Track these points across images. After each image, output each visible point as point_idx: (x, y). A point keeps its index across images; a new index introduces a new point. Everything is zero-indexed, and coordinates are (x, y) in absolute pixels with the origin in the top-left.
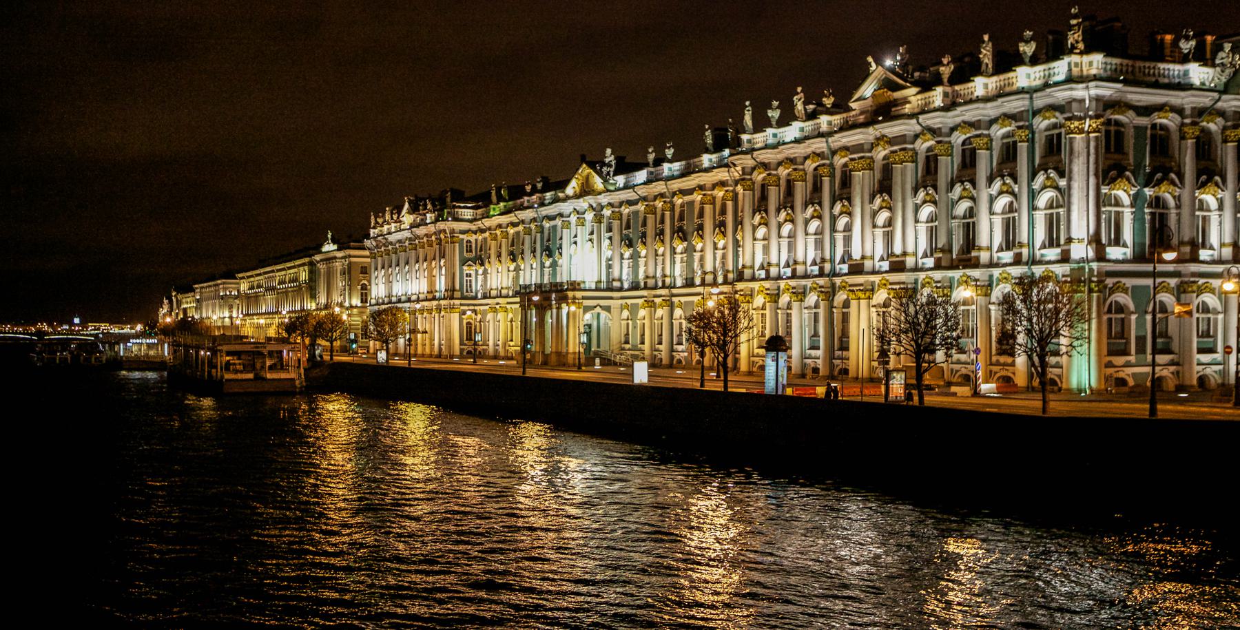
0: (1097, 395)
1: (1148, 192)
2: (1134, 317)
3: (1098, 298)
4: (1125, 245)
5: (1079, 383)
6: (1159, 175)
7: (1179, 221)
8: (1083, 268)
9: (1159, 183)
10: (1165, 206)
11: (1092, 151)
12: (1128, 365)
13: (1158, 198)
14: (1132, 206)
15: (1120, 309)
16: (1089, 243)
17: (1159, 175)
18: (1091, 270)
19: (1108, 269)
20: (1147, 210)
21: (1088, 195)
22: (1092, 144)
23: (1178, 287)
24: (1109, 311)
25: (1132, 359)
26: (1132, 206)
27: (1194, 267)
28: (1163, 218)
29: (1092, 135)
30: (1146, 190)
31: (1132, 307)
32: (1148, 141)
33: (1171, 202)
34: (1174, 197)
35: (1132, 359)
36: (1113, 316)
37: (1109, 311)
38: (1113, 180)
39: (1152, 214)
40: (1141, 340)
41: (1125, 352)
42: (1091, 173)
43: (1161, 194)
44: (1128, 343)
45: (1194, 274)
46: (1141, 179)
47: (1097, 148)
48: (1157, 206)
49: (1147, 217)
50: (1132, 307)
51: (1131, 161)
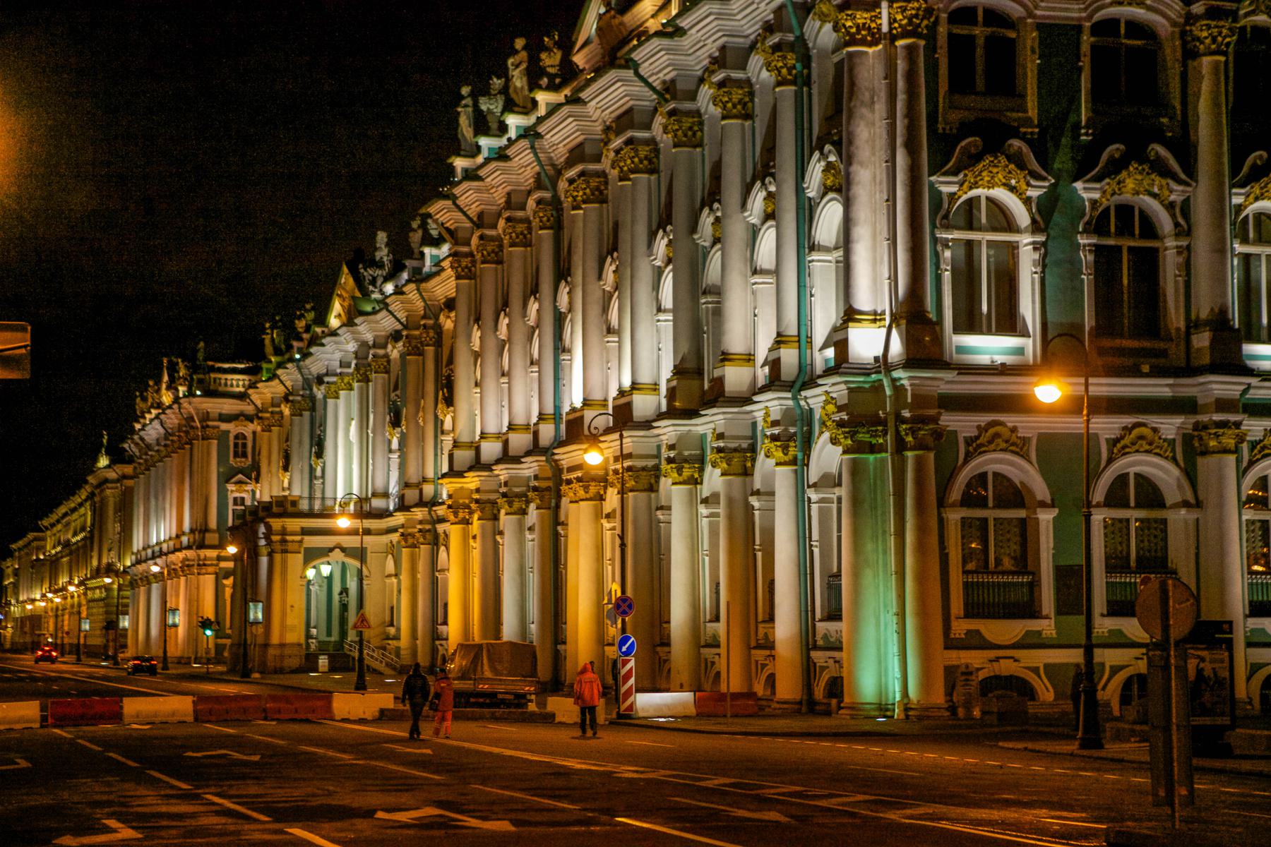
0: (920, 725)
1: (1086, 192)
2: (1046, 517)
3: (920, 463)
4: (1025, 334)
5: (882, 689)
6: (1115, 149)
7: (1187, 267)
8: (877, 388)
9: (1115, 168)
10: (1149, 228)
11: (901, 84)
12: (1032, 642)
13: (1125, 211)
14: (1035, 228)
15: (1013, 495)
16: (895, 318)
17: (1115, 149)
18: (898, 389)
19: (944, 388)
20: (1083, 240)
21: (892, 199)
22: (901, 65)
23: (1187, 439)
24: (970, 500)
25: (1047, 627)
26: (1035, 228)
27: (1223, 386)
28: (1148, 263)
29: (900, 43)
30: (1079, 185)
31: (1040, 489)
32: (1085, 63)
33: (1165, 221)
34: (1170, 207)
35: (1047, 627)
36: (990, 514)
37: (970, 500)
38: (972, 160)
39: (1098, 250)
40: (1072, 582)
41: (1030, 610)
42: (899, 141)
43: (1127, 197)
44: (1034, 586)
45: (1223, 405)
46: (1062, 161)
47: (911, 76)
48: (1125, 228)
49: (1087, 258)
50: (1040, 489)
51: (1033, 112)
